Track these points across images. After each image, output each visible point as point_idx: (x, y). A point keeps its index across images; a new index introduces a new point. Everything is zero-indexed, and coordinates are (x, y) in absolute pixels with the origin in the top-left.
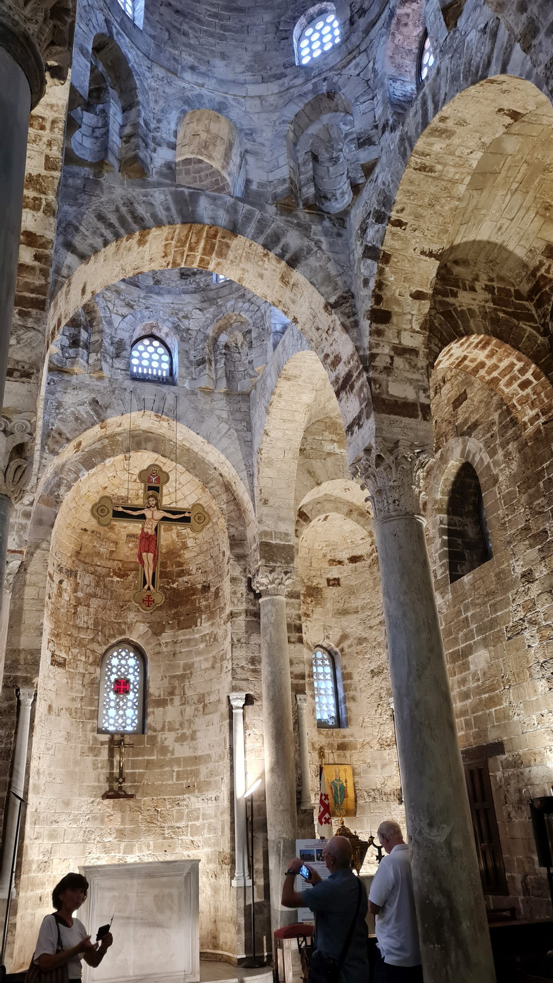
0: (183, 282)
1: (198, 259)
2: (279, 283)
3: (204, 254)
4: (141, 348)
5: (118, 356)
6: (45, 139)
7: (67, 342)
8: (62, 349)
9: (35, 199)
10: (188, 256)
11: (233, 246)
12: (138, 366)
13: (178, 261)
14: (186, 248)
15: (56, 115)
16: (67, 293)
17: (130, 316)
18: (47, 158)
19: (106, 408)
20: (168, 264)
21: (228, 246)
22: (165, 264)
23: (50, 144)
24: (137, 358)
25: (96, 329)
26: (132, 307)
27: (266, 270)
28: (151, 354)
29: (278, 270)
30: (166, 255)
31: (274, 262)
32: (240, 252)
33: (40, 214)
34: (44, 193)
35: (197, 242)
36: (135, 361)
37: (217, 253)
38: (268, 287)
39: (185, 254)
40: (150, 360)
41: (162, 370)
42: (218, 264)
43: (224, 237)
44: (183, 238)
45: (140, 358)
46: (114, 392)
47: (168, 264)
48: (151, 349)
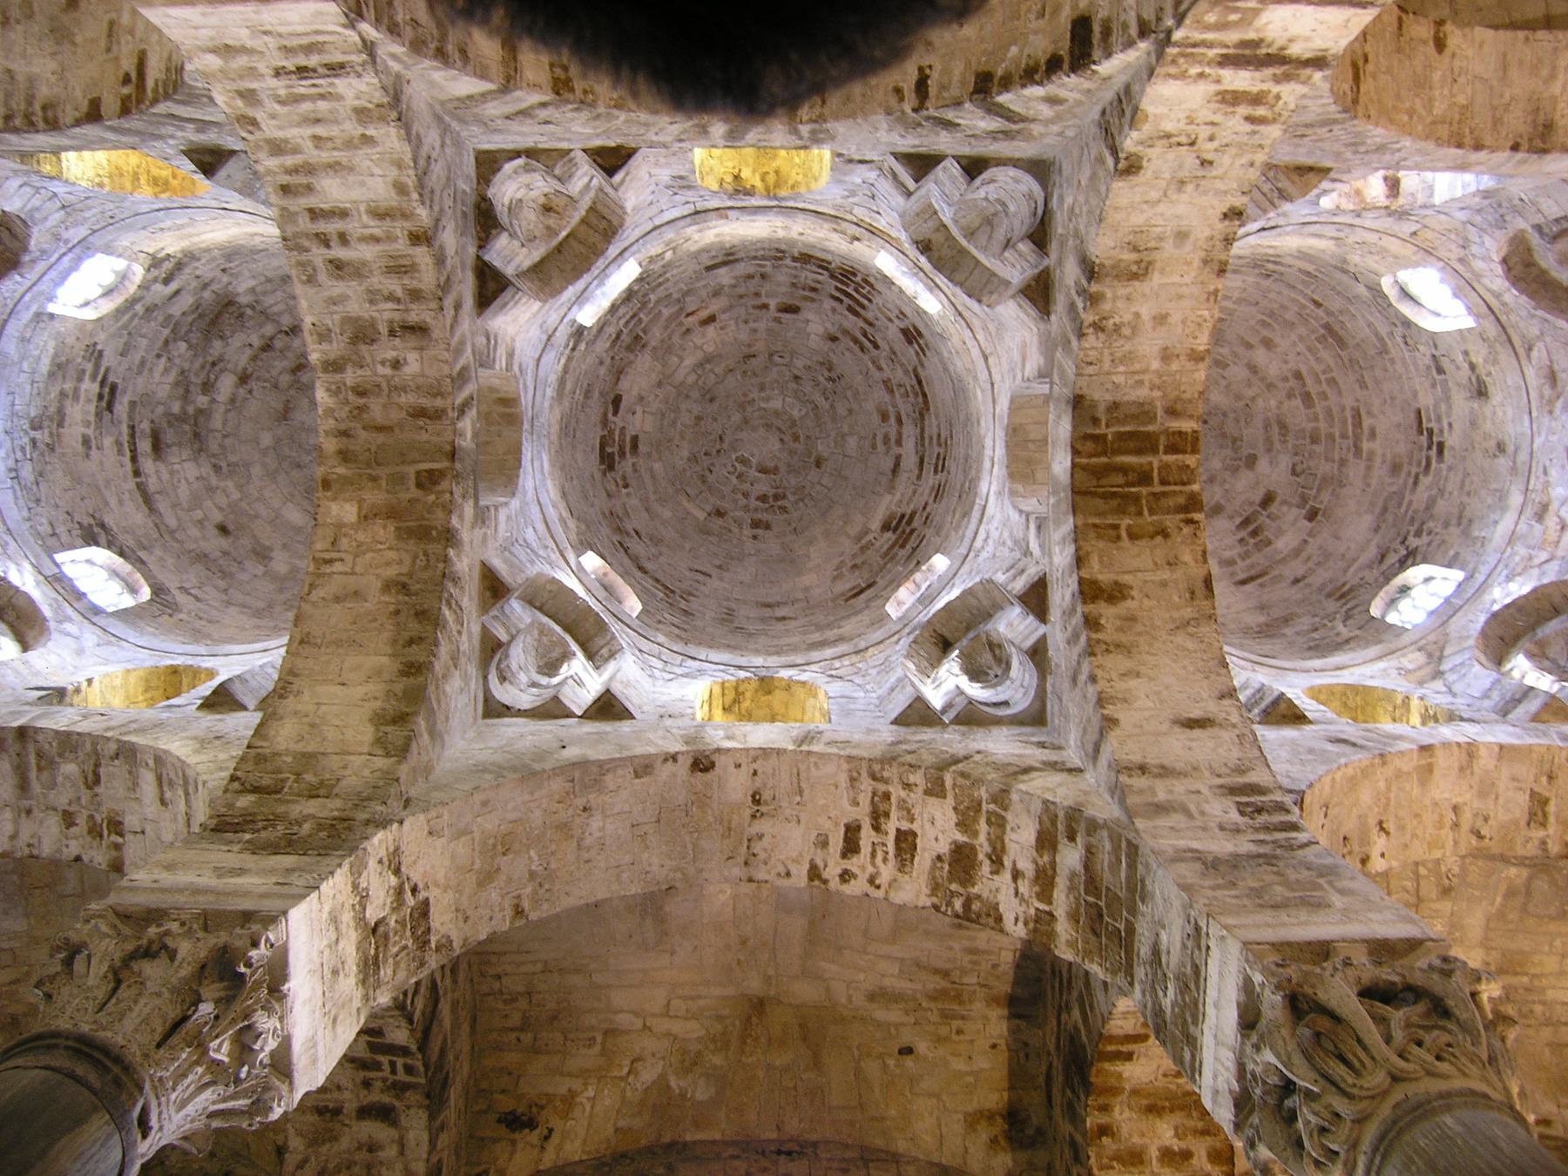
0: (1491, 389)
1: (1171, 458)
2: (1156, 279)
3: (1154, 450)
6: (903, 794)
9: (989, 822)
10: (1163, 482)
11: (1108, 397)
13: (1181, 500)
14: (1144, 491)
15: (864, 774)
16: (1165, 772)
17: (1563, 513)
18: (928, 792)
20: (1190, 522)
21: (1114, 406)
22: (1187, 530)
23: (907, 786)
27: (1137, 315)
29: (1121, 292)
30: (1164, 534)
31: (1106, 306)
32: (1119, 379)
33: (1009, 816)
34: (980, 805)
35: (1124, 470)
37: (1144, 424)
38: (1180, 297)
39: (1158, 488)
42: (1172, 412)
43: (1095, 421)
44: (1114, 503)
47: (1190, 522)
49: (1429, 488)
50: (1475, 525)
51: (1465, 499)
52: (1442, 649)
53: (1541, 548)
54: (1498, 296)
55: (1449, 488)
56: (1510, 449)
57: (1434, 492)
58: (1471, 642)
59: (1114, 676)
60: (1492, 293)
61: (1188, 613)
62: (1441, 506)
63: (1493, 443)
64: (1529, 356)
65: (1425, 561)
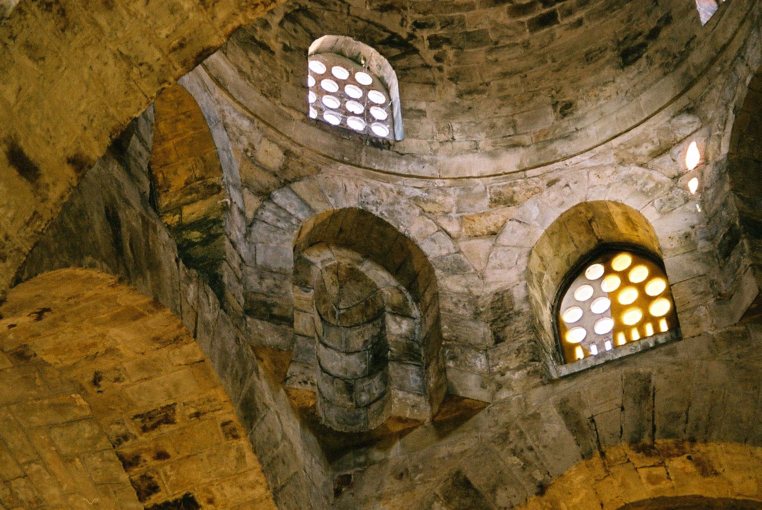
4: (581, 292)
5: (498, 340)
7: (356, 364)
8: (349, 388)
12: (585, 345)
17: (511, 225)
19: (493, 491)
24: (578, 324)
25: (428, 298)
26: (510, 201)
28: (613, 296)
36: (573, 336)
40: (616, 310)
41: (655, 321)
45: (588, 320)
46: (504, 438)
48: (612, 283)
49: (496, 27)
50: (465, 119)
51: (494, 85)
52: (298, 178)
53: (462, 220)
54: (741, 55)
55: (503, 56)
56: (568, 124)
57: (492, 36)
58: (322, 208)
59: (21, 39)
60: (743, 48)
61: (153, 56)
62: (478, 55)
63: (569, 95)
64: (680, 112)
65: (403, 74)
